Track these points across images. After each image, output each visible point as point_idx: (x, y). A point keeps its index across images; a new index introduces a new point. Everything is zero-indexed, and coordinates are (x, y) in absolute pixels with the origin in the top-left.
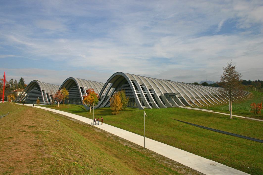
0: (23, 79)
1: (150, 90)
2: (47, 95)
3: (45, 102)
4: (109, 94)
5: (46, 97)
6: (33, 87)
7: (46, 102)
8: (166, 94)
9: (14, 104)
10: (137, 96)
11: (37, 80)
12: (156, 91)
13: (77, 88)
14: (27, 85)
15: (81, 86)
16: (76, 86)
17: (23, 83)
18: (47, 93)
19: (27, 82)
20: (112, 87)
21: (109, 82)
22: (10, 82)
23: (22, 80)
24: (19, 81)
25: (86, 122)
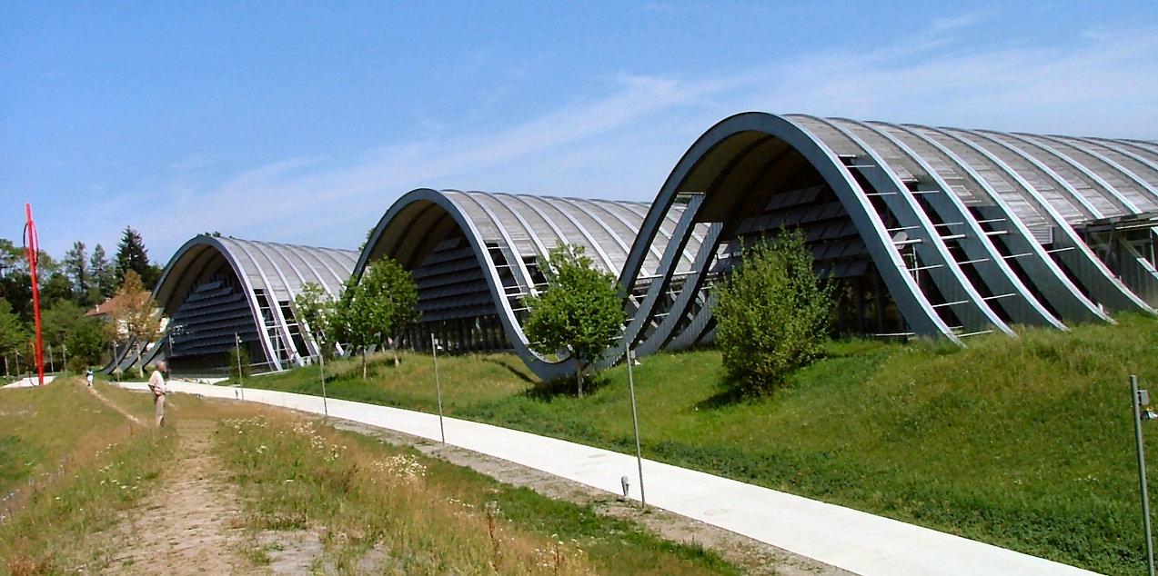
1: (976, 212)
2: (287, 313)
3: (276, 361)
4: (683, 269)
7: (284, 355)
8: (1092, 231)
9: (102, 390)
10: (898, 261)
11: (218, 235)
12: (1014, 210)
14: (164, 270)
16: (457, 240)
17: (142, 258)
18: (286, 303)
19: (160, 254)
22: (67, 262)
23: (132, 250)
24: (117, 250)
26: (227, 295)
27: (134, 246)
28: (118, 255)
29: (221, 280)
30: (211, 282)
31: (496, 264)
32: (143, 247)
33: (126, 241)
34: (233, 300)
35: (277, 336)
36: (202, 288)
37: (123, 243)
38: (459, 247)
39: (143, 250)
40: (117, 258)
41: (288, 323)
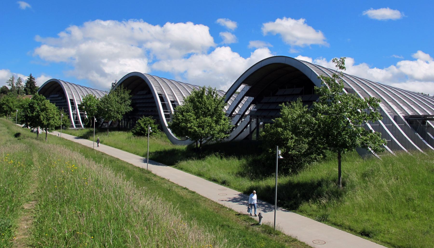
5: (77, 113)
8: (408, 118)
15: (160, 92)
20: (246, 95)
21: (243, 82)
25: (223, 190)
29: (58, 94)
30: (55, 94)
34: (62, 101)
35: (75, 116)
36: (52, 96)
38: (146, 94)
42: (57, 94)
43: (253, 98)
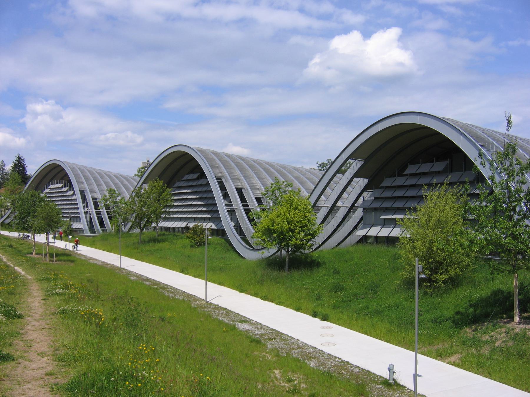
0: (23, 160)
2: (96, 205)
6: (51, 180)
13: (201, 182)
17: (24, 169)
18: (96, 199)
23: (20, 165)
24: (12, 165)
26: (65, 191)
27: (21, 164)
28: (12, 167)
29: (62, 183)
30: (57, 184)
31: (221, 190)
32: (25, 165)
33: (17, 161)
36: (52, 186)
37: (15, 162)
38: (198, 179)
39: (25, 166)
40: (11, 168)
41: (95, 209)
42: (60, 183)
43: (367, 180)
